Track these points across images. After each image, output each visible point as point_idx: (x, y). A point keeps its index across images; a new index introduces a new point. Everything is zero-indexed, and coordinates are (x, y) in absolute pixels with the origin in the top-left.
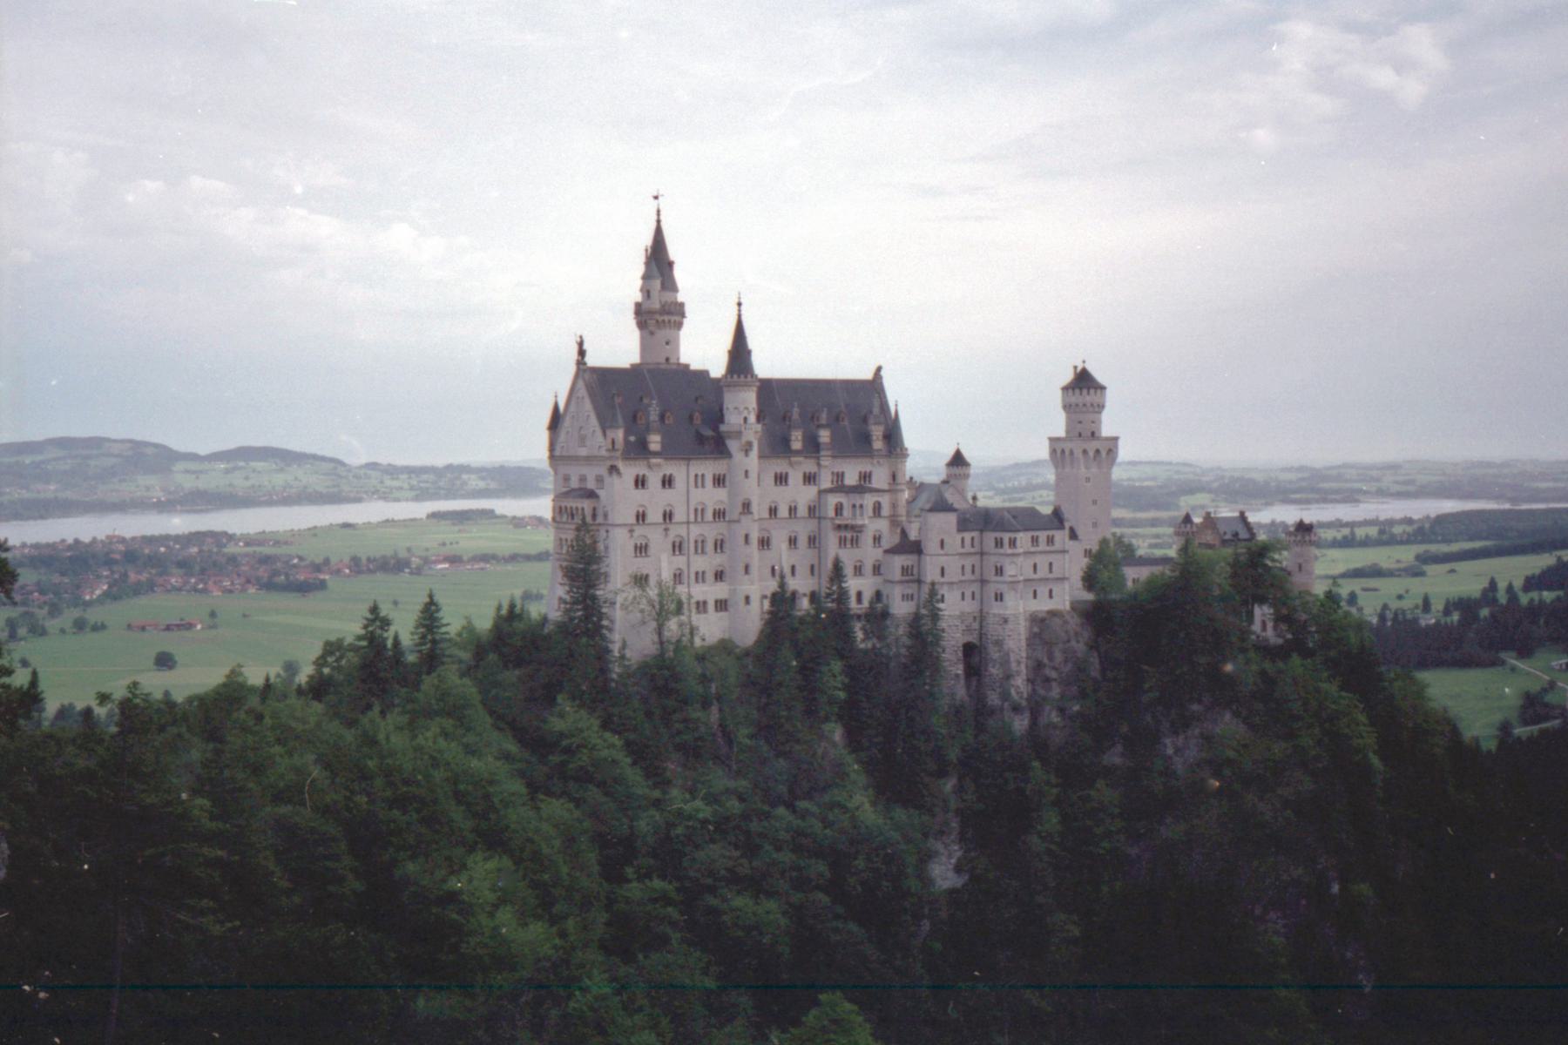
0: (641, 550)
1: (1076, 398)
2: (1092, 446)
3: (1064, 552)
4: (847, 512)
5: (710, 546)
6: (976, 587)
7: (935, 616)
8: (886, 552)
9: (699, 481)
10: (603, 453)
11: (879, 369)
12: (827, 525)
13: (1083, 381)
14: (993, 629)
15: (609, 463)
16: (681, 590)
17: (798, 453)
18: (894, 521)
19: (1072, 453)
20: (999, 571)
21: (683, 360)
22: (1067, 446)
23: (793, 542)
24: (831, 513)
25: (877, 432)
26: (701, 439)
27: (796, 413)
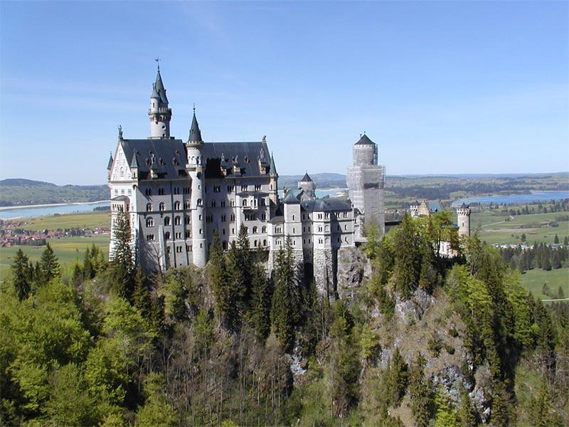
4: (248, 204)
7: (290, 250)
10: (132, 180)
16: (169, 242)
21: (171, 136)
24: (242, 205)
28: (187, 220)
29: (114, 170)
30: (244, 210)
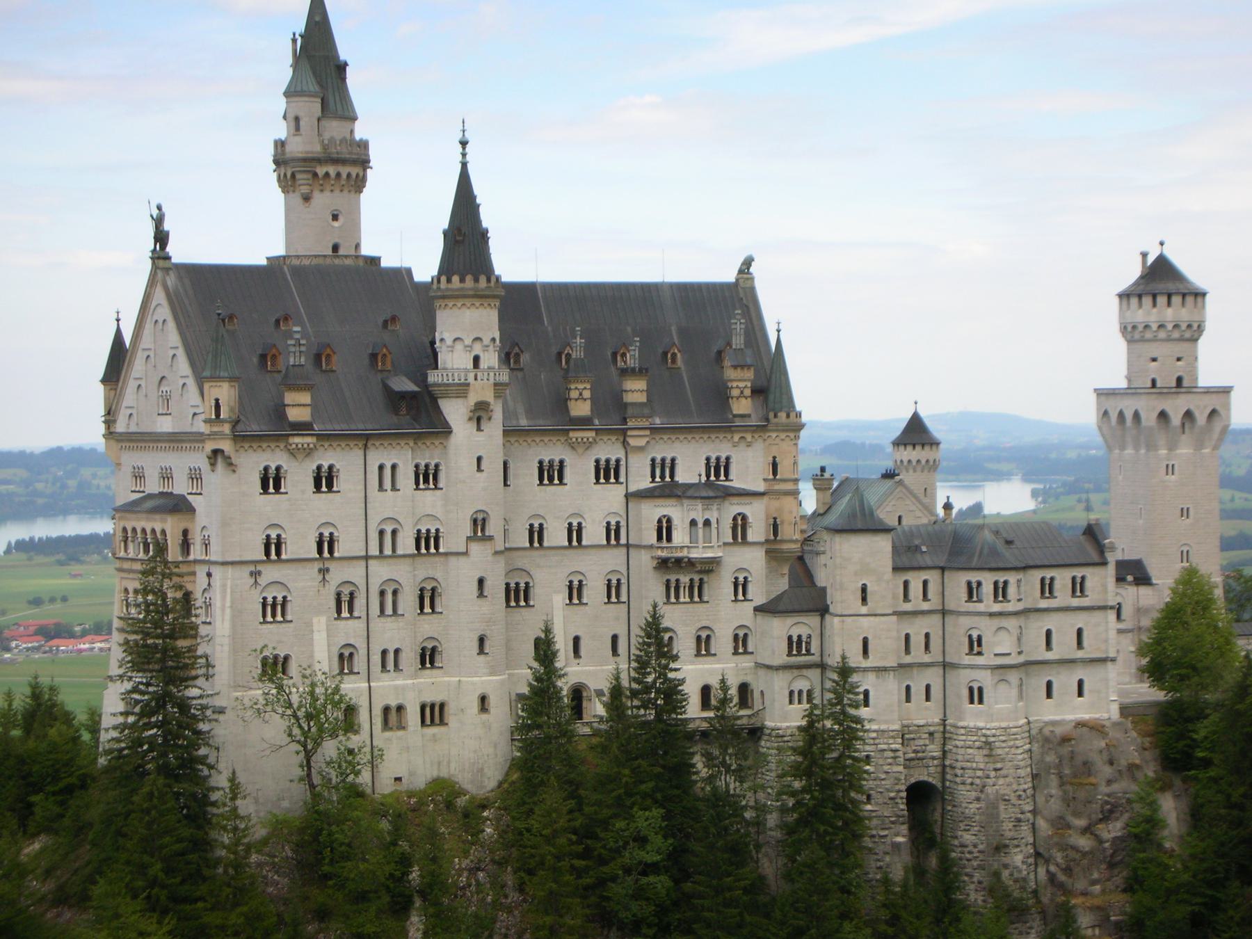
0: (274, 609)
1: (1144, 313)
2: (1176, 407)
3: (1103, 608)
5: (408, 601)
6: (933, 677)
7: (850, 731)
8: (757, 609)
9: (387, 478)
10: (202, 428)
11: (748, 262)
12: (644, 562)
13: (1160, 279)
14: (967, 756)
15: (210, 446)
17: (584, 422)
18: (774, 553)
19: (1136, 415)
20: (975, 645)
21: (366, 250)
22: (1129, 405)
23: (575, 591)
25: (740, 381)
26: (396, 400)
27: (577, 350)
28: (428, 598)
29: (131, 386)
30: (664, 564)
